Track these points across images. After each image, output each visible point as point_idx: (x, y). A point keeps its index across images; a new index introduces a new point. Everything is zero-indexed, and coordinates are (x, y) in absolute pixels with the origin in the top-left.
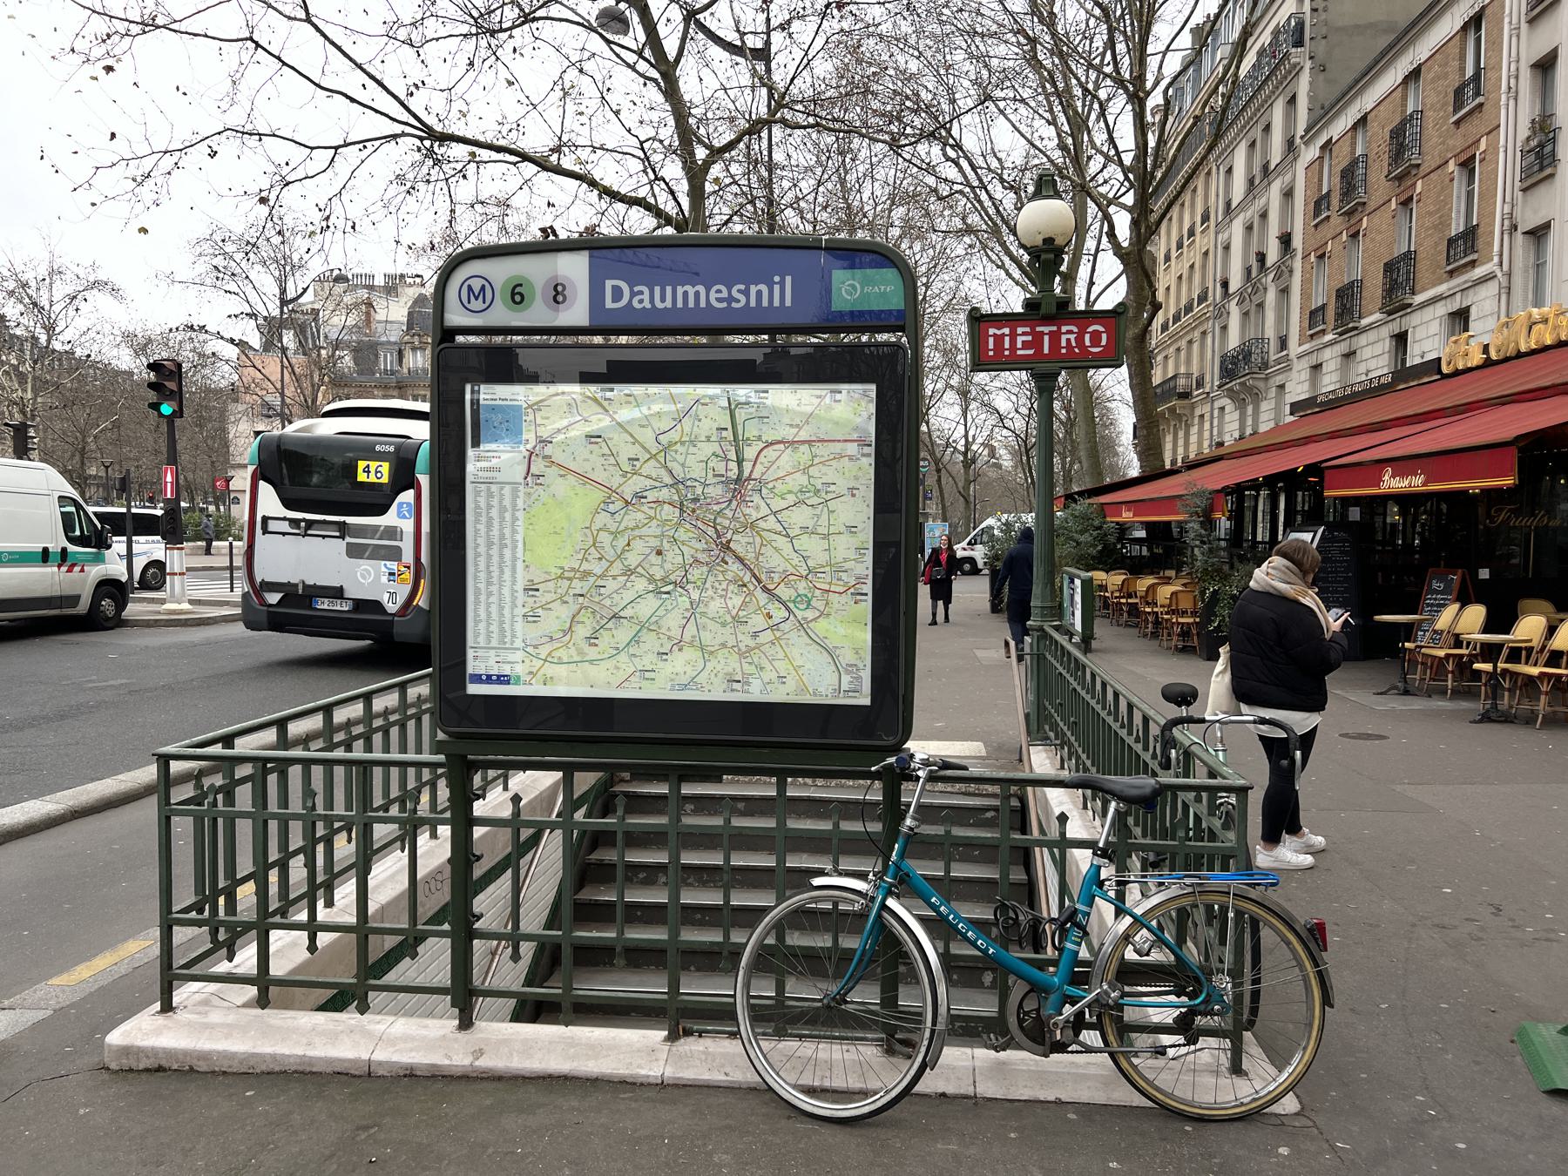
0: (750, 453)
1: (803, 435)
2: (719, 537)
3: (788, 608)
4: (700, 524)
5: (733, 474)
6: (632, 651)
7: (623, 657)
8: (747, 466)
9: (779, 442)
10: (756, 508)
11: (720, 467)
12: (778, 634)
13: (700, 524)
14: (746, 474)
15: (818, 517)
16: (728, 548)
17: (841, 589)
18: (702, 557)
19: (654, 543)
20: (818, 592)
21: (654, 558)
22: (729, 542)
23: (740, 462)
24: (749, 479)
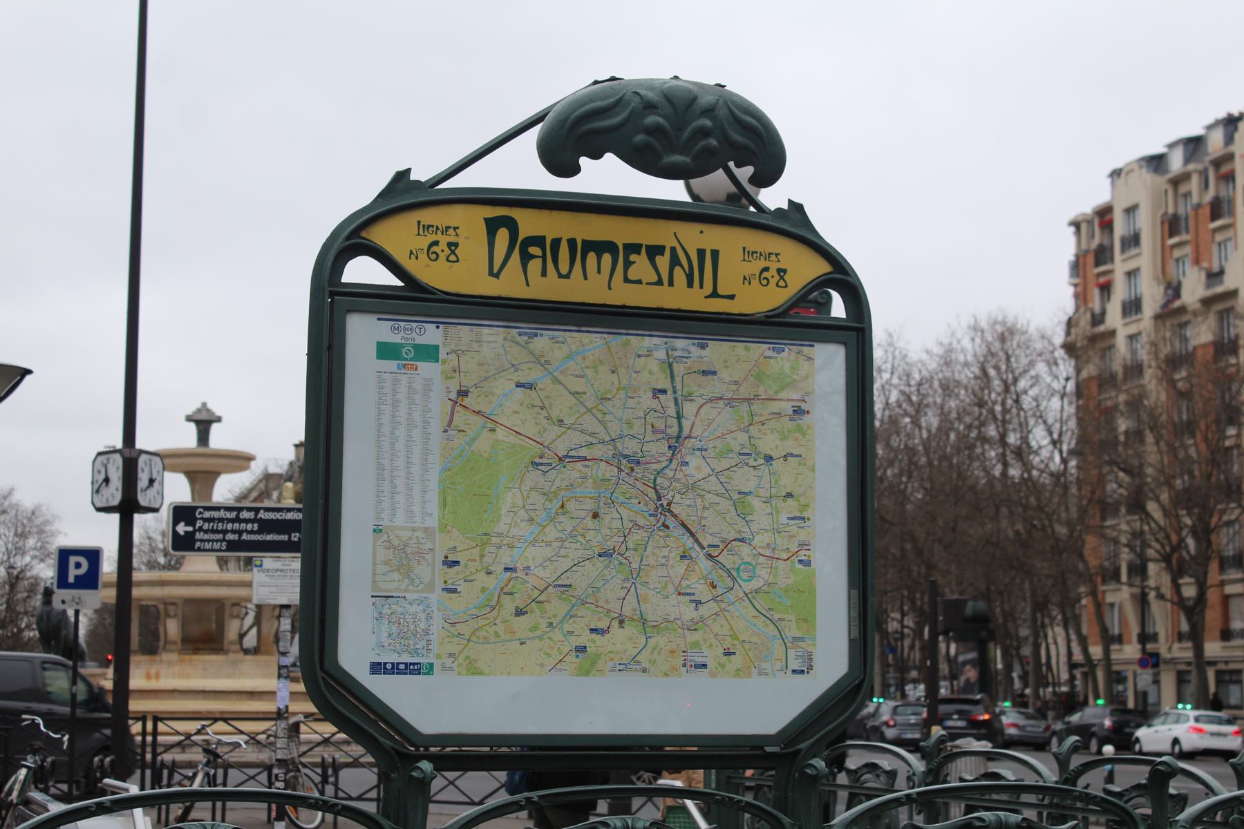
0: (689, 409)
1: (744, 391)
2: (659, 498)
3: (734, 579)
4: (639, 484)
5: (673, 431)
6: (567, 627)
7: (557, 635)
8: (686, 424)
9: (721, 398)
10: (696, 467)
11: (660, 424)
12: (723, 605)
13: (639, 484)
14: (686, 432)
15: (760, 477)
16: (670, 511)
17: (785, 556)
18: (641, 522)
19: (590, 505)
20: (761, 559)
21: (589, 522)
22: (669, 504)
23: (679, 417)
24: (689, 437)
